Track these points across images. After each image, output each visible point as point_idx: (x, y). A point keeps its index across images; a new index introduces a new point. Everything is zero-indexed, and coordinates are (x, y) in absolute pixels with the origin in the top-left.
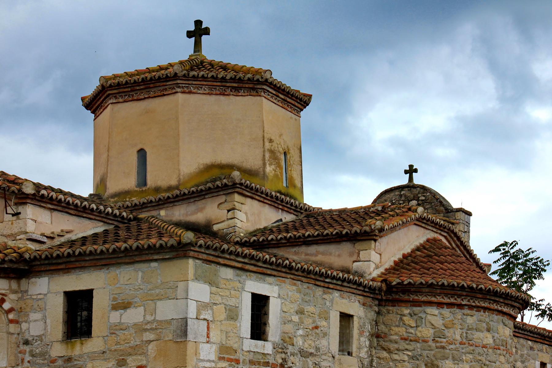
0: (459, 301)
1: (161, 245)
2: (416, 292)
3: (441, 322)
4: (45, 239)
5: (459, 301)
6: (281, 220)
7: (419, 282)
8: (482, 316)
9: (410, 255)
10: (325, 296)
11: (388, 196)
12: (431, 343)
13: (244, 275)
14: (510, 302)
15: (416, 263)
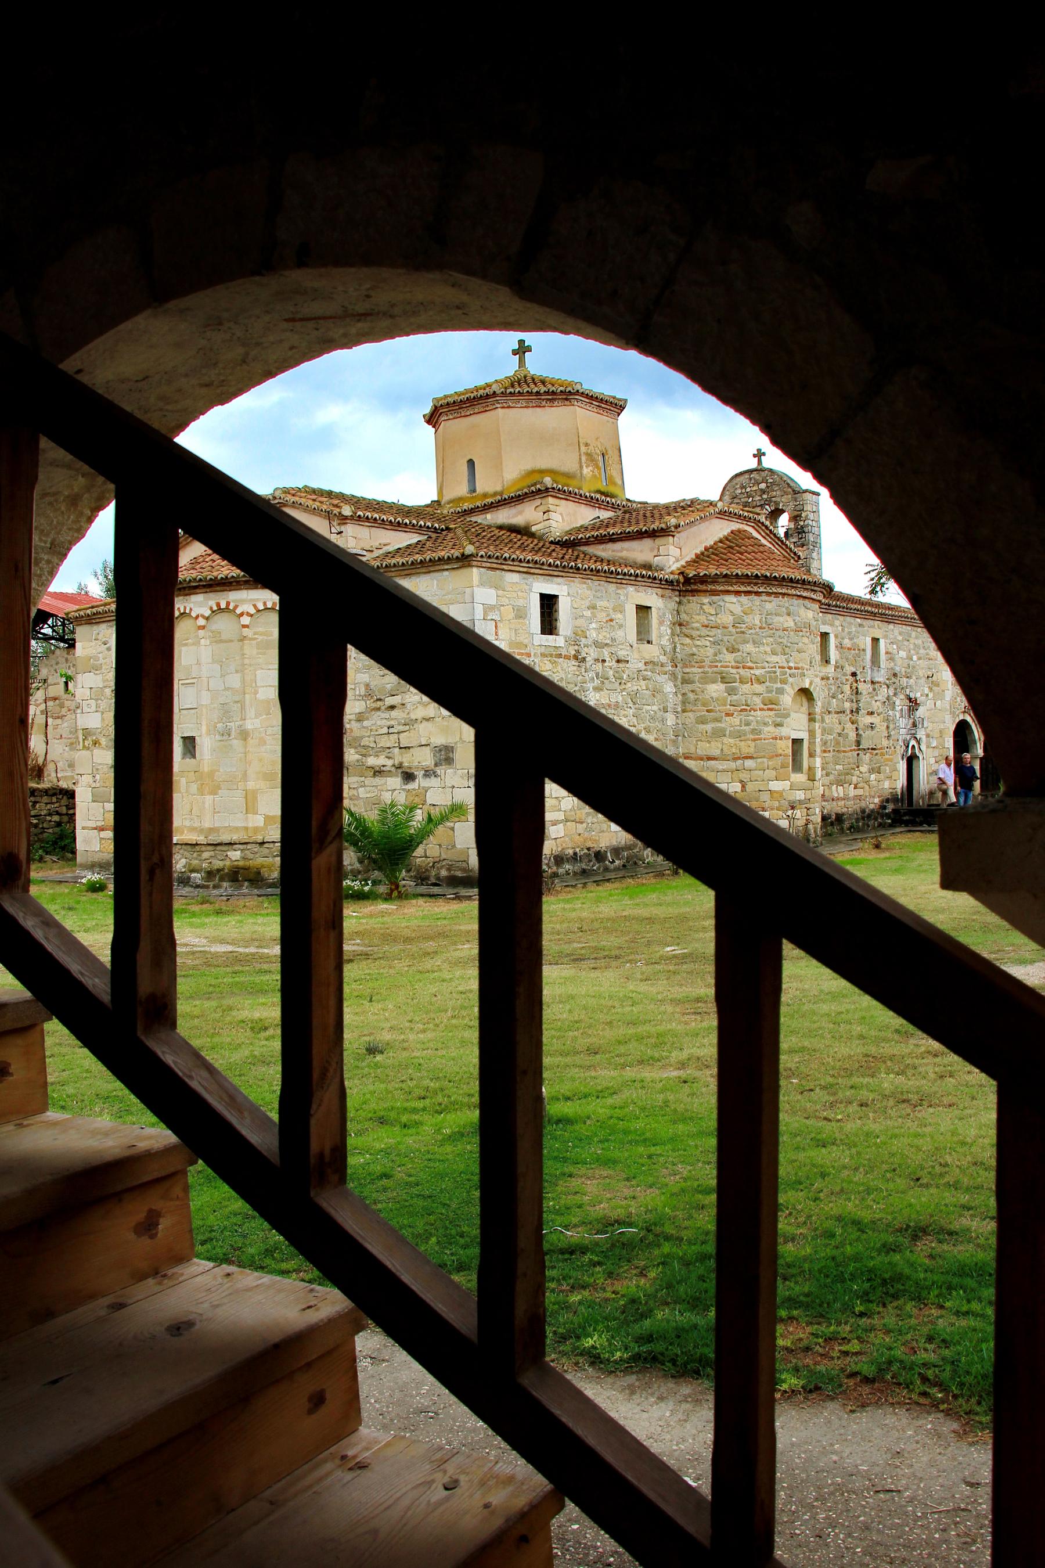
0: (756, 589)
1: (449, 557)
2: (713, 582)
3: (740, 609)
4: (365, 553)
5: (756, 589)
6: (599, 517)
7: (714, 573)
9: (712, 547)
10: (619, 591)
11: (738, 479)
12: (731, 629)
13: (531, 578)
14: (809, 587)
15: (716, 555)
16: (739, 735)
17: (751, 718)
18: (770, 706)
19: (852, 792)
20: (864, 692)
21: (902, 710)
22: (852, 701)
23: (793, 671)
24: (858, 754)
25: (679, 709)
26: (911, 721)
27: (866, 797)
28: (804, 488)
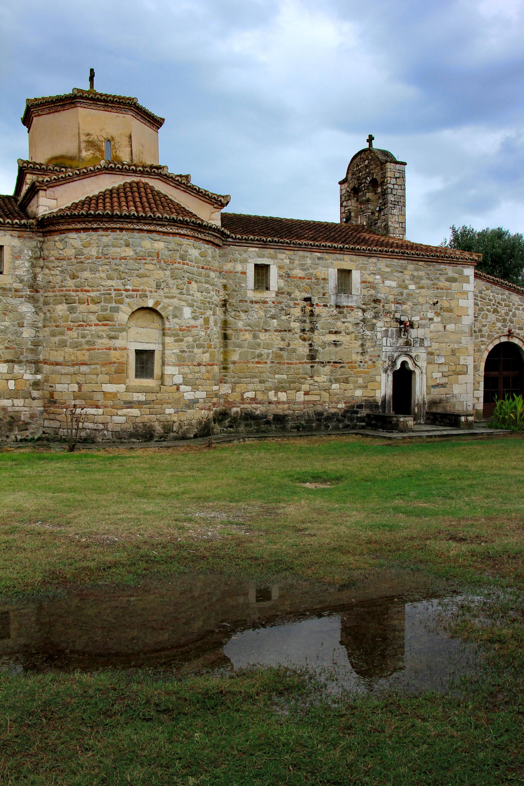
0: (90, 225)
2: (58, 224)
3: (80, 243)
5: (90, 225)
8: (119, 235)
12: (74, 261)
16: (76, 346)
17: (86, 332)
18: (105, 322)
19: (300, 397)
20: (323, 315)
21: (387, 331)
22: (305, 322)
23: (130, 293)
24: (312, 367)
25: (40, 325)
26: (401, 341)
27: (325, 402)
28: (398, 160)
